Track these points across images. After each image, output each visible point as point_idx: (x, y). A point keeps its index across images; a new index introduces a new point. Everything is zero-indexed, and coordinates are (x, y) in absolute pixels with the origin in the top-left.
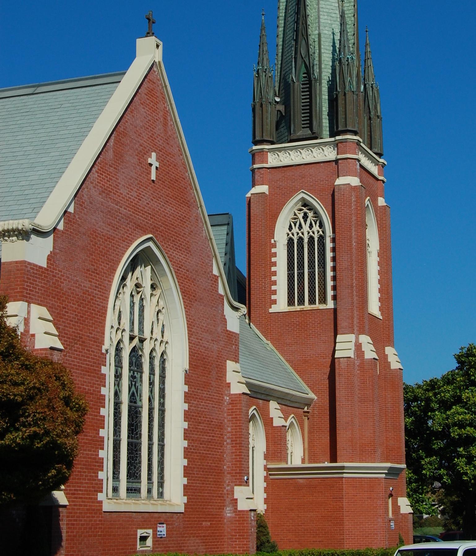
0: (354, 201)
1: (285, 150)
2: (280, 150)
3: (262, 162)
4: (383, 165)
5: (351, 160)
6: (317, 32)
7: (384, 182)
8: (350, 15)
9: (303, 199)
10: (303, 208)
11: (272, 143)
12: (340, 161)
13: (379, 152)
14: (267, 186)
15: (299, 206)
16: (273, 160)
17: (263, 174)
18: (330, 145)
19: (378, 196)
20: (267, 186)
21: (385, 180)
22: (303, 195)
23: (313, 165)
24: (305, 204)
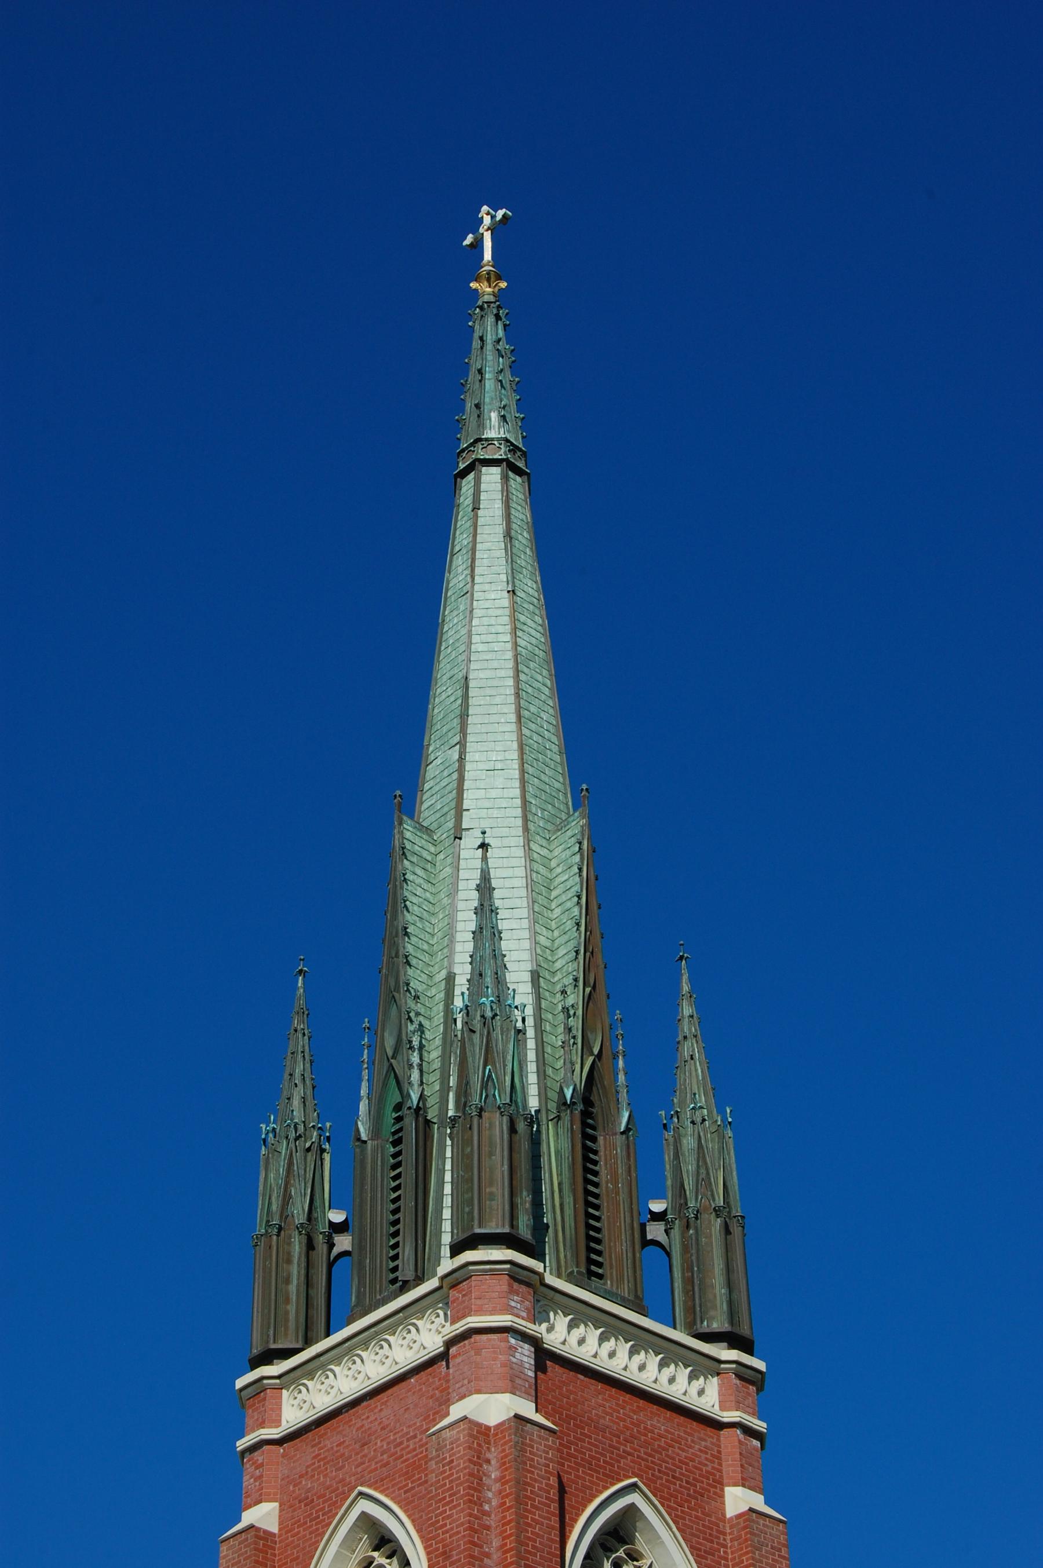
0: (497, 1480)
1: (323, 1367)
2: (307, 1370)
3: (262, 1425)
4: (746, 1376)
5: (484, 1337)
6: (443, 974)
7: (750, 1432)
8: (569, 904)
9: (364, 1515)
10: (376, 1554)
11: (287, 1354)
12: (453, 1350)
13: (726, 1327)
14: (275, 1505)
15: (364, 1548)
16: (293, 1411)
17: (262, 1465)
18: (433, 1306)
19: (719, 1484)
20: (276, 1505)
21: (760, 1425)
22: (364, 1506)
23: (390, 1391)
24: (384, 1541)
